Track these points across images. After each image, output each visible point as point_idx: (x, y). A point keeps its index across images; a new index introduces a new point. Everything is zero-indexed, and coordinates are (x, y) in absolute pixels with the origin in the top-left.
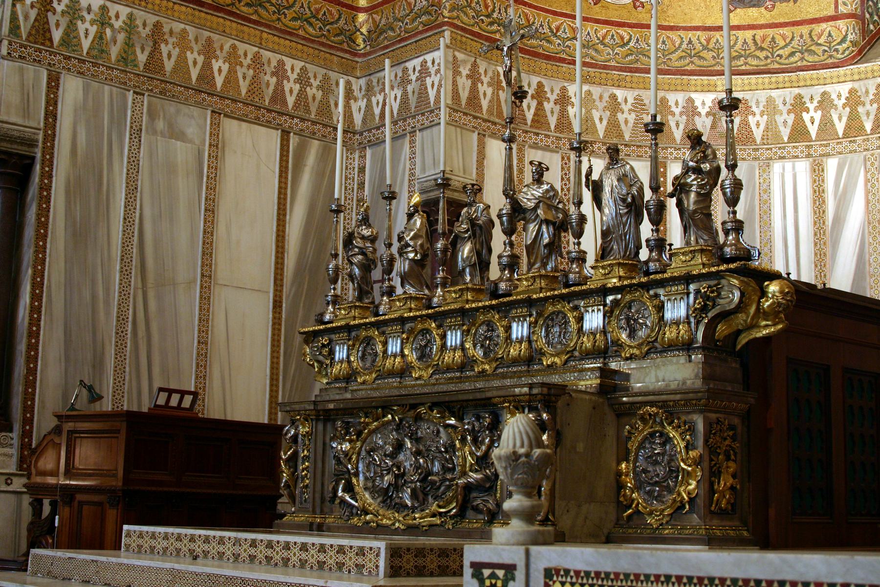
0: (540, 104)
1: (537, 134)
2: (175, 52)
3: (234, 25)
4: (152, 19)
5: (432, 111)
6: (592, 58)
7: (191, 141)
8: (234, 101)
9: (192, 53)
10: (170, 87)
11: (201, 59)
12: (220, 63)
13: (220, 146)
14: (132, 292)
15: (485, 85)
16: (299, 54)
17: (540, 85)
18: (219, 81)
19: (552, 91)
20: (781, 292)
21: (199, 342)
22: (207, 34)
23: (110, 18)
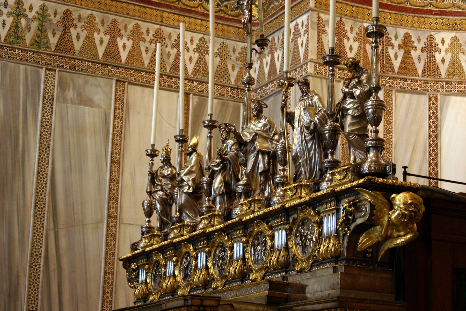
0: (407, 53)
1: (405, 80)
2: (84, 34)
3: (137, 8)
4: (62, 9)
5: (301, 67)
6: (459, 7)
7: (98, 106)
8: (138, 71)
9: (99, 34)
10: (78, 62)
11: (106, 39)
12: (125, 40)
13: (124, 109)
14: (44, 232)
15: (351, 40)
16: (198, 28)
17: (407, 37)
18: (124, 55)
19: (419, 40)
20: (405, 204)
21: (105, 272)
22: (112, 17)
23: (25, 10)
